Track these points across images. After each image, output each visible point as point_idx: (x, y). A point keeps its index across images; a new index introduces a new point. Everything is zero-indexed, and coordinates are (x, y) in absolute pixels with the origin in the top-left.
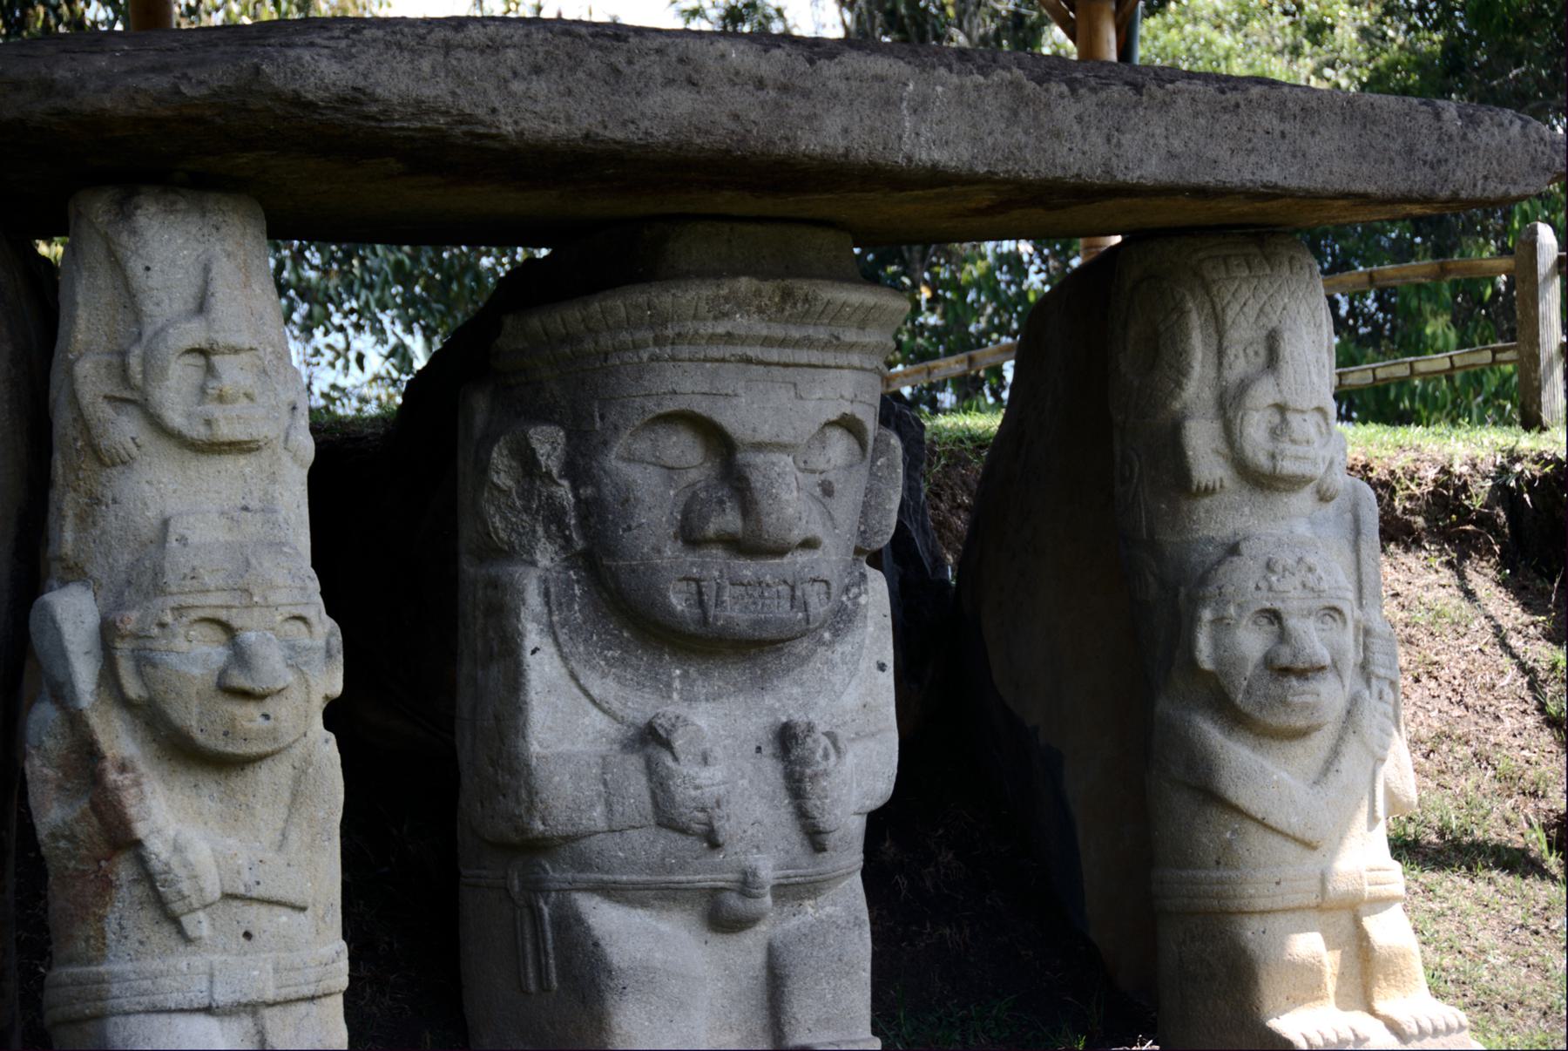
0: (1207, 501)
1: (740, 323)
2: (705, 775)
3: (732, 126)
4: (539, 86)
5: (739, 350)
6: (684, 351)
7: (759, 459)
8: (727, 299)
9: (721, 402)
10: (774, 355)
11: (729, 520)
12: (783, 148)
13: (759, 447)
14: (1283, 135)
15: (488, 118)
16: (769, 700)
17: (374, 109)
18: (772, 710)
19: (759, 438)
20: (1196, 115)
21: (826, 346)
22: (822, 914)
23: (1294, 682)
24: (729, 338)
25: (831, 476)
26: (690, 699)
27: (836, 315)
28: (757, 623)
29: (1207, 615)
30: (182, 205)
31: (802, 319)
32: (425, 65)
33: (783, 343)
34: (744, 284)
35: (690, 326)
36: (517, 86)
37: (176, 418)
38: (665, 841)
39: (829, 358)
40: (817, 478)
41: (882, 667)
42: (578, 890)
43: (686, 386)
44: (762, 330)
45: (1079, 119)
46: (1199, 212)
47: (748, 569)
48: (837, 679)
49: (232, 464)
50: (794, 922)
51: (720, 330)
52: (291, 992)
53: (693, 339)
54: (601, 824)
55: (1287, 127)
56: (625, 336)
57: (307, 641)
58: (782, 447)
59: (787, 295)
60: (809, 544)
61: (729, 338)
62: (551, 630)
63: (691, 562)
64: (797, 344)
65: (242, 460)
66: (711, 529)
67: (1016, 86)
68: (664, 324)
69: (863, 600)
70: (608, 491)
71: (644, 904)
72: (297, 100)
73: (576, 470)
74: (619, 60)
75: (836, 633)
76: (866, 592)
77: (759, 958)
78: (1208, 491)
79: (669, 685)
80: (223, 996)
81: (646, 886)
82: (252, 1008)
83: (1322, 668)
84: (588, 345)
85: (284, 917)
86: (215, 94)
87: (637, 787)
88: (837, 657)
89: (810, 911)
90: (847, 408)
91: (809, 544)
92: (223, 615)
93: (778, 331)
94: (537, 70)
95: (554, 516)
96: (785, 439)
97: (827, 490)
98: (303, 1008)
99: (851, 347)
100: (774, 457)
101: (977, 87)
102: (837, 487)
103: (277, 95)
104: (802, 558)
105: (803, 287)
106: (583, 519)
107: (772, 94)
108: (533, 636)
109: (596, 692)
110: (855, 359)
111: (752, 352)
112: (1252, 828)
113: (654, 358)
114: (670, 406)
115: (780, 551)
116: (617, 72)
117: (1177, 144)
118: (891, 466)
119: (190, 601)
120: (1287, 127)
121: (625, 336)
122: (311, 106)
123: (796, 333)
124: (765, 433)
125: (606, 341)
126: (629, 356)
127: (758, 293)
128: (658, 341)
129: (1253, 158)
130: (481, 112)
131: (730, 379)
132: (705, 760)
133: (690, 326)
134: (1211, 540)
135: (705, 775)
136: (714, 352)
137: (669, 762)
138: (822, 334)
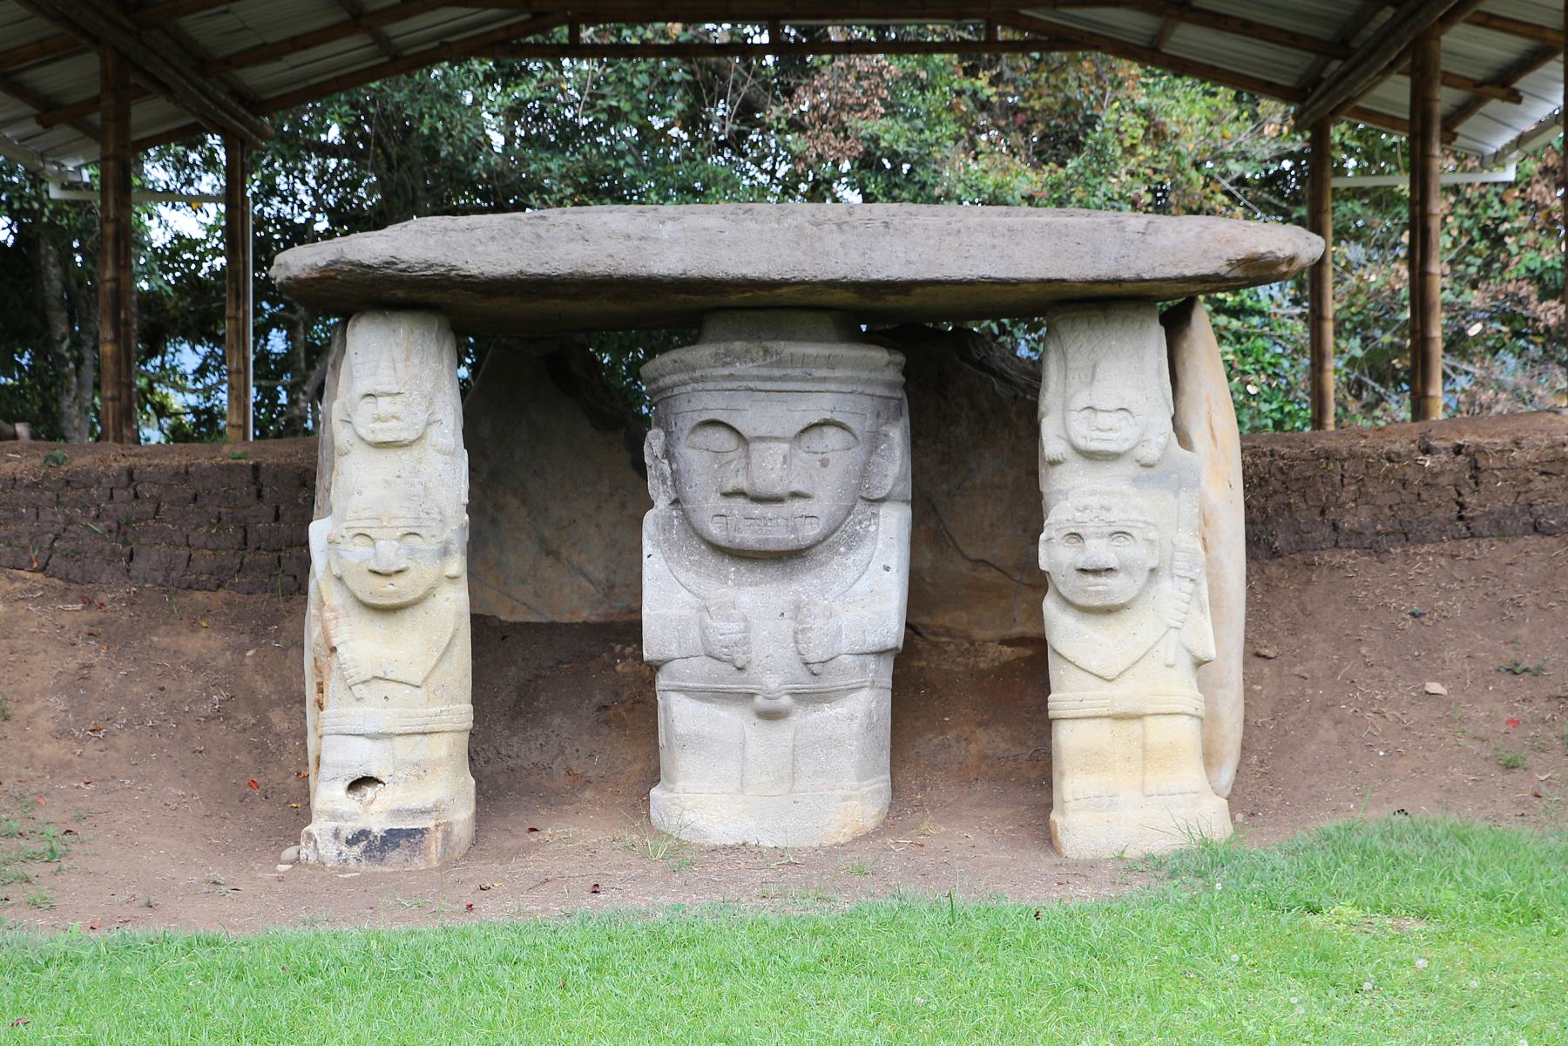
0: (1059, 468)
1: (739, 368)
2: (726, 627)
3: (609, 261)
4: (493, 247)
5: (744, 384)
6: (710, 385)
7: (763, 446)
8: (726, 355)
9: (735, 414)
10: (768, 386)
11: (741, 482)
12: (644, 272)
13: (762, 439)
14: (994, 247)
15: (465, 267)
16: (794, 586)
17: (403, 266)
18: (796, 592)
19: (758, 434)
20: (928, 238)
21: (804, 380)
22: (833, 713)
23: (1091, 578)
24: (731, 377)
25: (829, 456)
26: (739, 584)
27: (805, 361)
28: (759, 541)
29: (1043, 537)
30: (380, 319)
31: (780, 363)
32: (432, 241)
33: (771, 379)
34: (738, 346)
35: (708, 372)
36: (480, 249)
37: (362, 432)
38: (710, 664)
39: (808, 386)
40: (819, 456)
41: (887, 569)
42: (679, 690)
43: (712, 405)
44: (755, 372)
45: (842, 245)
46: (1116, 289)
47: (757, 510)
48: (850, 576)
49: (392, 456)
50: (815, 715)
51: (726, 372)
52: (408, 729)
53: (714, 379)
54: (676, 655)
55: (996, 242)
56: (675, 378)
57: (423, 547)
58: (777, 439)
59: (766, 351)
60: (795, 495)
61: (731, 377)
62: (657, 545)
63: (724, 505)
64: (783, 378)
65: (400, 452)
66: (729, 488)
67: (799, 228)
68: (694, 369)
69: (872, 528)
70: (682, 466)
71: (709, 701)
72: (361, 265)
73: (668, 454)
74: (541, 231)
75: (850, 548)
76: (877, 525)
77: (790, 735)
78: (1054, 463)
79: (726, 577)
80: (370, 729)
81: (704, 691)
82: (388, 736)
83: (1110, 569)
84: (661, 383)
85: (407, 690)
86: (328, 265)
87: (695, 633)
88: (849, 562)
89: (829, 712)
90: (828, 416)
91: (795, 495)
92: (367, 532)
93: (765, 372)
94: (493, 239)
95: (664, 483)
96: (776, 434)
97: (824, 463)
98: (419, 738)
99: (825, 380)
100: (772, 445)
101: (772, 231)
102: (833, 462)
103: (351, 263)
104: (798, 506)
105: (774, 346)
106: (674, 481)
107: (636, 242)
108: (647, 547)
109: (682, 580)
110: (833, 387)
111: (751, 385)
112: (1072, 667)
113: (694, 390)
114: (706, 416)
115: (778, 500)
116: (539, 236)
117: (913, 256)
118: (890, 448)
119: (351, 524)
120: (996, 242)
121: (675, 378)
122: (369, 267)
123: (777, 373)
124: (763, 432)
125: (668, 381)
126: (682, 389)
127: (747, 351)
128: (695, 380)
129: (970, 261)
130: (459, 264)
131: (741, 400)
132: (728, 618)
133: (708, 372)
134: (1060, 491)
135: (726, 627)
136: (728, 385)
137: (709, 621)
138: (797, 372)
